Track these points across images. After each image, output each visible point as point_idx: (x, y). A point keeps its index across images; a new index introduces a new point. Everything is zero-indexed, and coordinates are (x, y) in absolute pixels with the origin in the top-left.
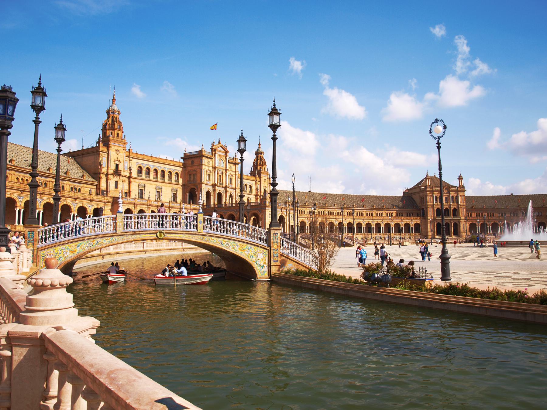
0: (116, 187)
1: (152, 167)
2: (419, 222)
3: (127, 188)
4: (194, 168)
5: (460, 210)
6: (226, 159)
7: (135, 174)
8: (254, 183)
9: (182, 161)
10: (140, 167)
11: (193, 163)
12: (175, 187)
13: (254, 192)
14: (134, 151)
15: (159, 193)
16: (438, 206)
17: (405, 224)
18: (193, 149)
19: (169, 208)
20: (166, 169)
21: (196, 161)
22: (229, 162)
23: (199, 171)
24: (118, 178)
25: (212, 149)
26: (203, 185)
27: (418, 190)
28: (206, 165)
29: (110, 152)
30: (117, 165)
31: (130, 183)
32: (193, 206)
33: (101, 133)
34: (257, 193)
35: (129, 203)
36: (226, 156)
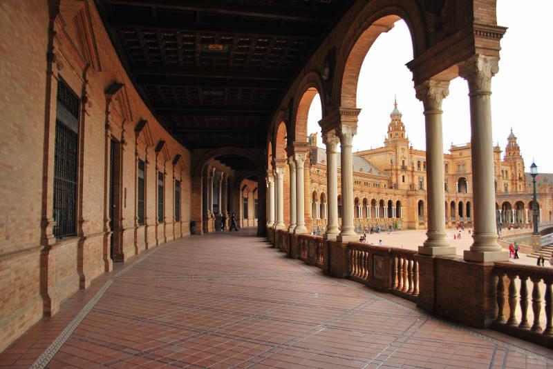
0: (403, 181)
3: (410, 181)
8: (509, 168)
9: (450, 153)
10: (419, 162)
11: (461, 154)
13: (510, 178)
14: (414, 148)
30: (403, 161)
31: (413, 176)
32: (466, 195)
33: (387, 135)
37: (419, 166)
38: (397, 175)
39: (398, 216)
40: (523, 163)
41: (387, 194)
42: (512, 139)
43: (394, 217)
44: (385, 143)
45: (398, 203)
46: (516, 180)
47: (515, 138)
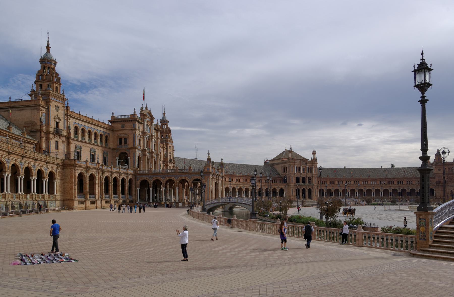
1: (86, 128)
2: (283, 187)
3: (65, 148)
4: (124, 132)
5: (314, 179)
6: (151, 124)
7: (73, 135)
8: (162, 149)
11: (123, 127)
15: (93, 158)
16: (298, 175)
17: (367, 190)
18: (124, 111)
19: (112, 172)
20: (99, 131)
21: (128, 126)
22: (154, 129)
23: (131, 135)
24: (58, 138)
25: (141, 114)
26: (137, 150)
27: (280, 161)
28: (138, 130)
29: (50, 108)
30: (57, 123)
31: (69, 144)
35: (82, 167)
36: (152, 122)
38: (48, 139)
41: (36, 160)
44: (30, 95)
45: (51, 175)
47: (167, 122)
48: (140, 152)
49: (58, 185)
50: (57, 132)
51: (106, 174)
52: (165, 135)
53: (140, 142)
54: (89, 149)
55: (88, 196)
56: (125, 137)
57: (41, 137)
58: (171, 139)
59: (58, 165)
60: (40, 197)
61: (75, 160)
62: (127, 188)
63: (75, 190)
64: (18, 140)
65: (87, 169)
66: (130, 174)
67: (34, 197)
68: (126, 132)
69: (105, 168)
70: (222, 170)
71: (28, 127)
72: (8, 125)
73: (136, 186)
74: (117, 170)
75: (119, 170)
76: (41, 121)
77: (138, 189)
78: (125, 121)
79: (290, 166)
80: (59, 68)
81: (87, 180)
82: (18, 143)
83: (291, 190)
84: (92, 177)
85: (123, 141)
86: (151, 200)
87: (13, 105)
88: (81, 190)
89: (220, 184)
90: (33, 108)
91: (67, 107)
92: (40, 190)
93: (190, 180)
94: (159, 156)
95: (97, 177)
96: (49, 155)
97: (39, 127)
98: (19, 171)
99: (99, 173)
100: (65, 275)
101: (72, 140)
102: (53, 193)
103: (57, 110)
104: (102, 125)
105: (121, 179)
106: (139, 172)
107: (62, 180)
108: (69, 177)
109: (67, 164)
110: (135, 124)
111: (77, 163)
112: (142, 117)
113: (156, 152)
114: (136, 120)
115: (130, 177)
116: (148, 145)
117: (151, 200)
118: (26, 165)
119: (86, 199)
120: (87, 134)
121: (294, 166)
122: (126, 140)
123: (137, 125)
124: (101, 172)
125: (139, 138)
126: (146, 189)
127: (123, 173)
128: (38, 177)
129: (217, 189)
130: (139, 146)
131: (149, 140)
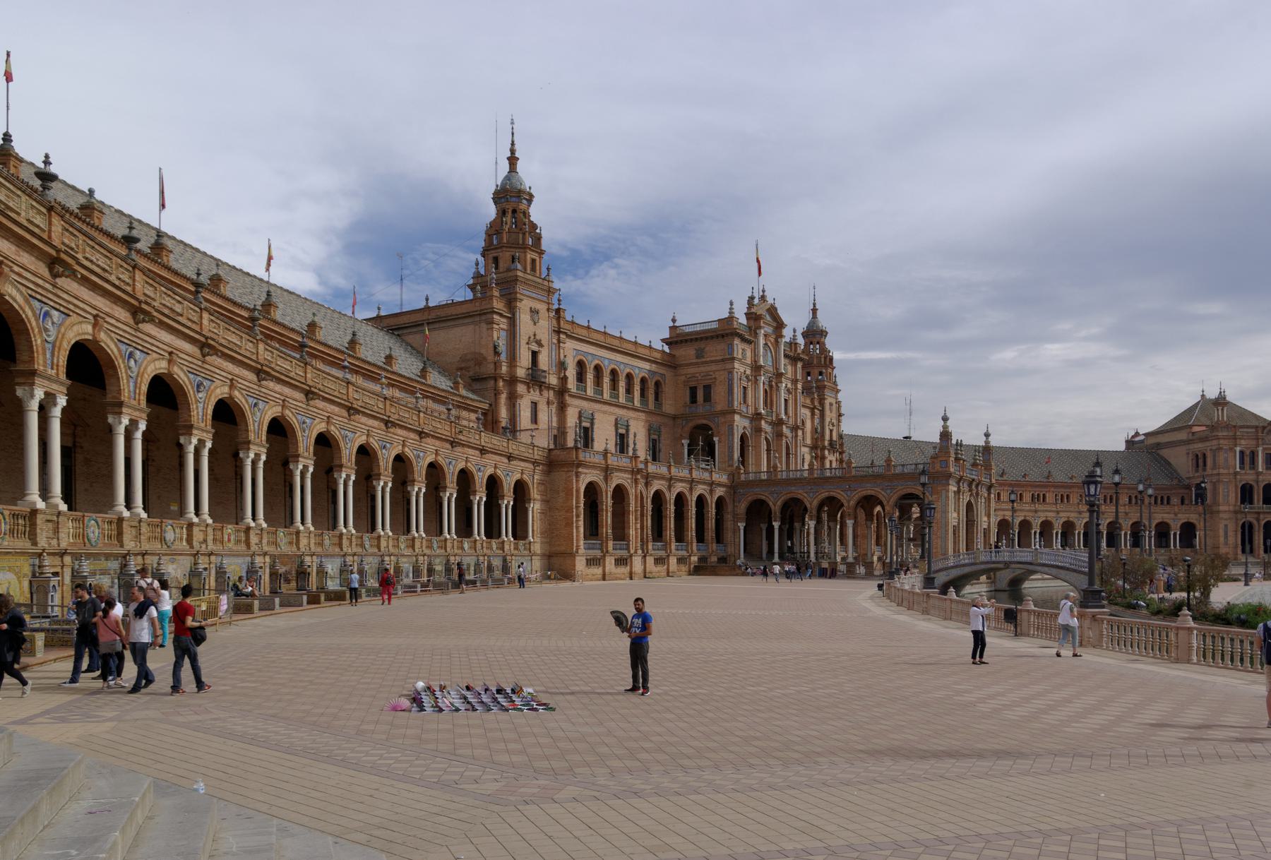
0: (535, 419)
1: (606, 362)
2: (1193, 518)
3: (555, 419)
4: (702, 369)
6: (777, 343)
8: (807, 412)
9: (666, 349)
11: (700, 354)
12: (656, 420)
13: (809, 441)
18: (701, 313)
19: (671, 479)
20: (637, 371)
21: (714, 350)
22: (786, 356)
23: (721, 376)
25: (749, 315)
26: (737, 417)
27: (1182, 436)
28: (740, 360)
30: (535, 355)
31: (562, 408)
34: (815, 440)
35: (594, 467)
37: (581, 377)
38: (513, 398)
39: (519, 531)
40: (838, 403)
41: (483, 451)
42: (814, 334)
43: (507, 537)
45: (521, 489)
46: (824, 448)
47: (823, 333)
48: (746, 423)
49: (537, 516)
50: (535, 379)
51: (657, 485)
52: (816, 371)
53: (745, 394)
54: (612, 419)
55: (611, 544)
56: (707, 382)
57: (497, 393)
58: (835, 383)
59: (535, 463)
60: (494, 547)
61: (577, 448)
62: (711, 524)
63: (577, 528)
64: (444, 403)
65: (607, 471)
66: (720, 485)
67: (479, 546)
68: (709, 369)
69: (652, 468)
70: (988, 467)
71: (466, 369)
72: (421, 366)
73: (736, 519)
74: (684, 473)
75: (691, 471)
76: (497, 353)
77: (742, 525)
78: (707, 338)
79: (1220, 449)
80: (536, 213)
81: (607, 502)
82: (443, 408)
83: (1222, 526)
84: (620, 493)
85: (699, 393)
86: (776, 555)
87: (433, 315)
88: (593, 529)
89: (980, 507)
90: (477, 319)
91: (558, 311)
92: (492, 530)
93: (889, 497)
94: (800, 433)
95: (632, 492)
96: (515, 438)
97: (492, 366)
98: (445, 478)
99: (636, 481)
100: (512, 746)
101: (571, 396)
102: (525, 537)
103: (533, 320)
104: (647, 352)
105: (695, 499)
106: (743, 477)
107: (546, 501)
108: (562, 494)
109: (556, 462)
110: (732, 345)
111: (582, 456)
112: (752, 323)
113: (791, 422)
114: (735, 334)
115: (720, 492)
116: (768, 402)
117: (776, 555)
118: (461, 465)
119: (605, 553)
120: (606, 380)
121: (1232, 450)
122: (707, 389)
123: (739, 347)
124: (642, 481)
125: (744, 384)
126: (764, 526)
127: (700, 480)
128: (487, 496)
129: (971, 523)
130: (744, 403)
131: (771, 386)
